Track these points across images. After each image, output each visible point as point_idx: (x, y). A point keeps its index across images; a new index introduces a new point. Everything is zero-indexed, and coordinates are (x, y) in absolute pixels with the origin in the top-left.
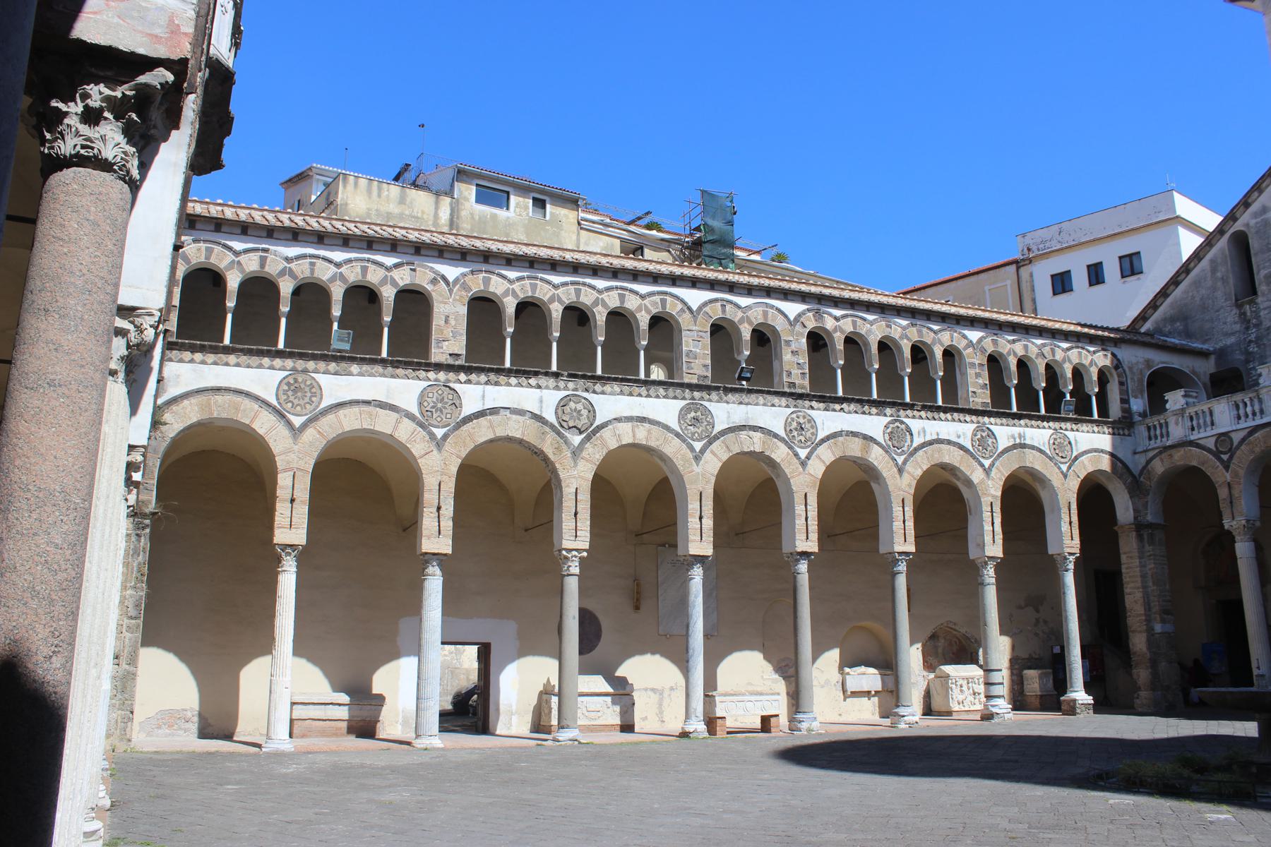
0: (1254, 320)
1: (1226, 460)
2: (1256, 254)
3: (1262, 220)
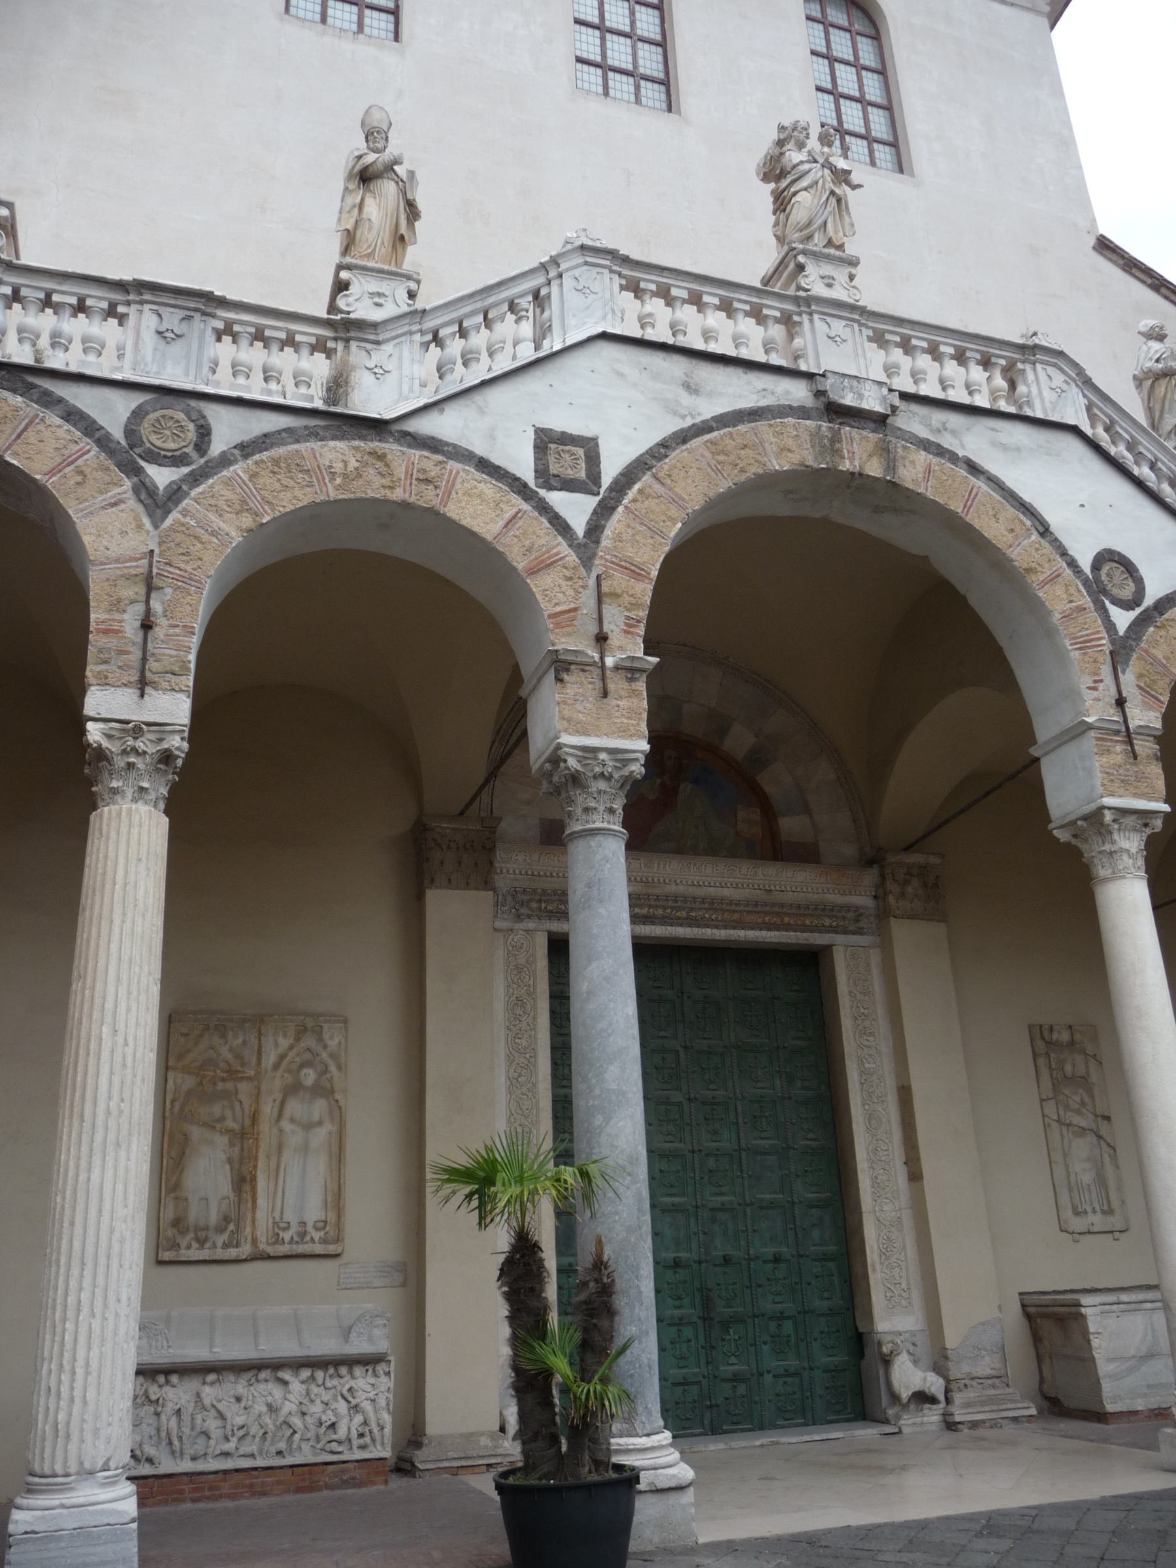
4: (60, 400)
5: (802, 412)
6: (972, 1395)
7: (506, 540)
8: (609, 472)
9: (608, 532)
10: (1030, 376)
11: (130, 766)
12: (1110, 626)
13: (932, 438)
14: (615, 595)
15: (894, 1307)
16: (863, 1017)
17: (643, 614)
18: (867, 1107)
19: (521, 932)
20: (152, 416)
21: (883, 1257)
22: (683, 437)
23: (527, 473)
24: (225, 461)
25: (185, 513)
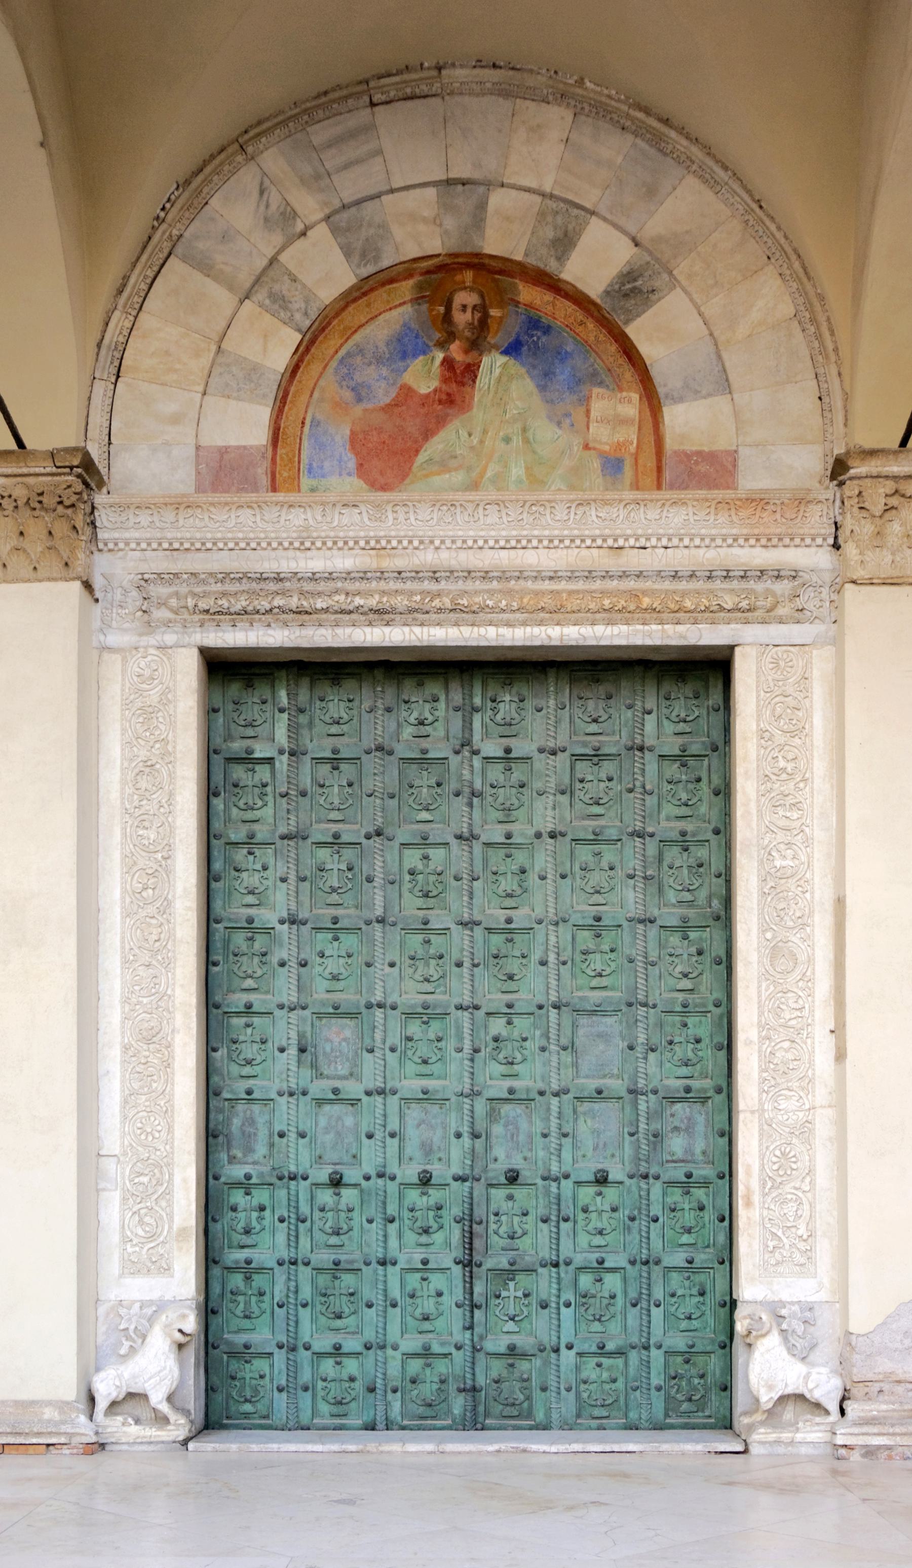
6: (884, 1407)
15: (778, 1263)
16: (784, 776)
18: (769, 935)
19: (152, 651)
21: (769, 1184)
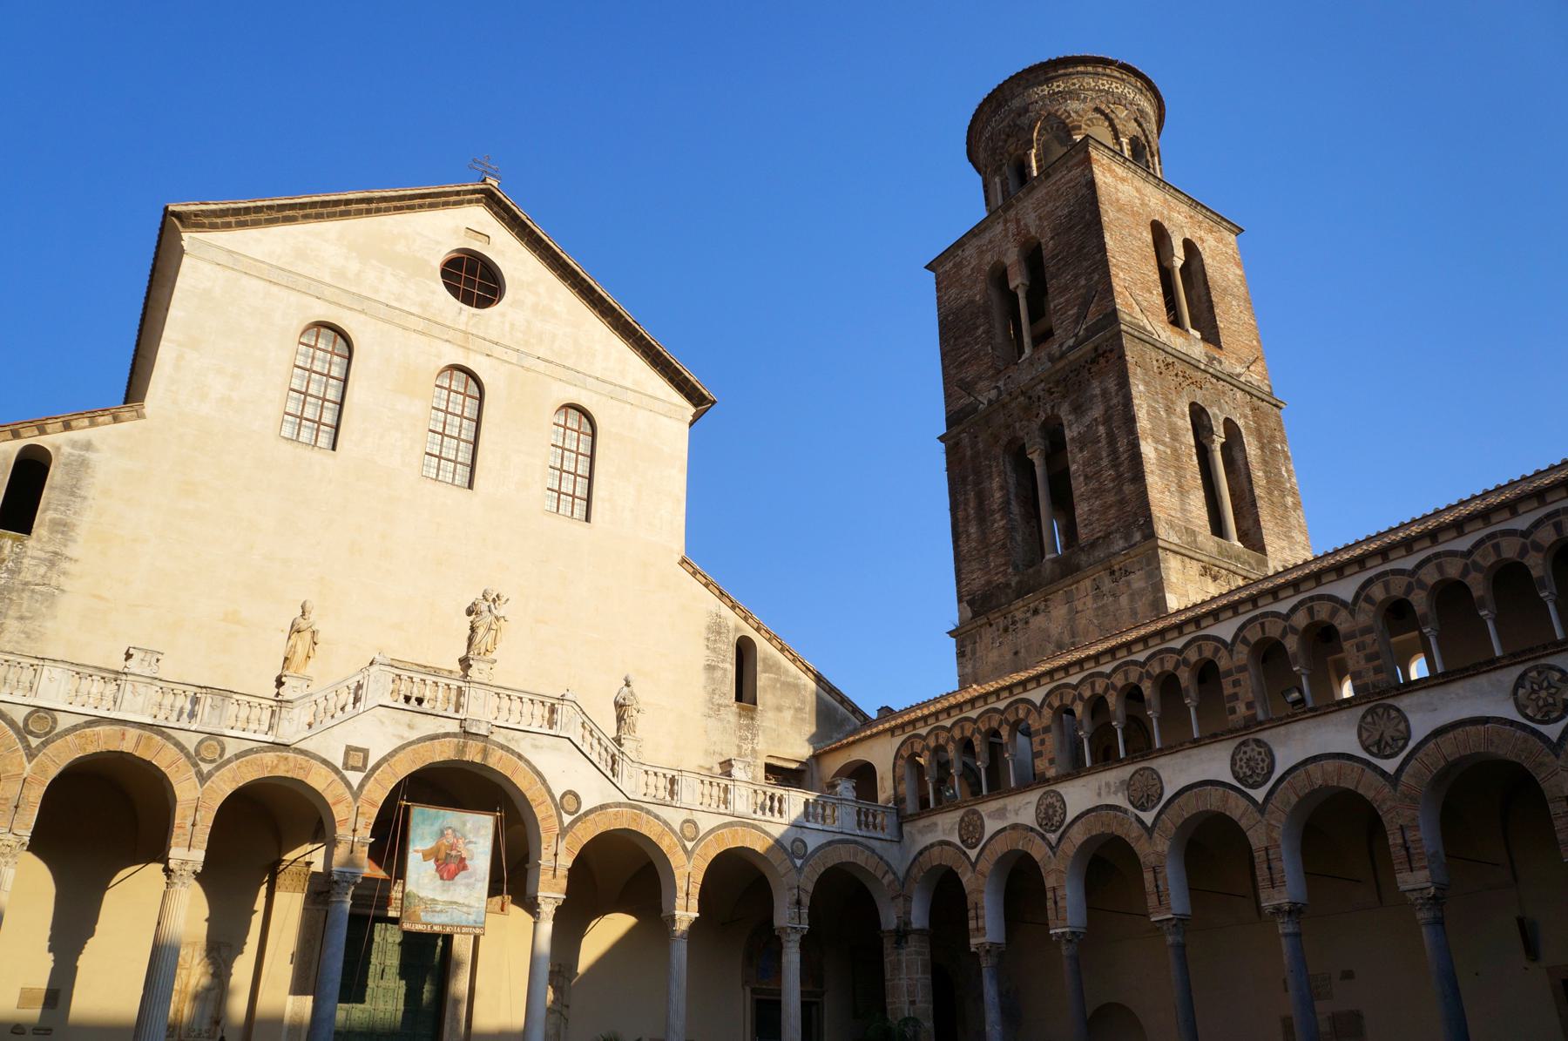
0: (11, 563)
1: (33, 745)
2: (52, 488)
3: (80, 456)
4: (174, 738)
5: (455, 735)
7: (326, 792)
8: (371, 763)
9: (366, 788)
10: (560, 711)
11: (181, 875)
12: (561, 822)
13: (506, 744)
14: (363, 814)
17: (373, 821)
20: (206, 744)
22: (402, 748)
23: (339, 764)
24: (229, 761)
25: (213, 782)
